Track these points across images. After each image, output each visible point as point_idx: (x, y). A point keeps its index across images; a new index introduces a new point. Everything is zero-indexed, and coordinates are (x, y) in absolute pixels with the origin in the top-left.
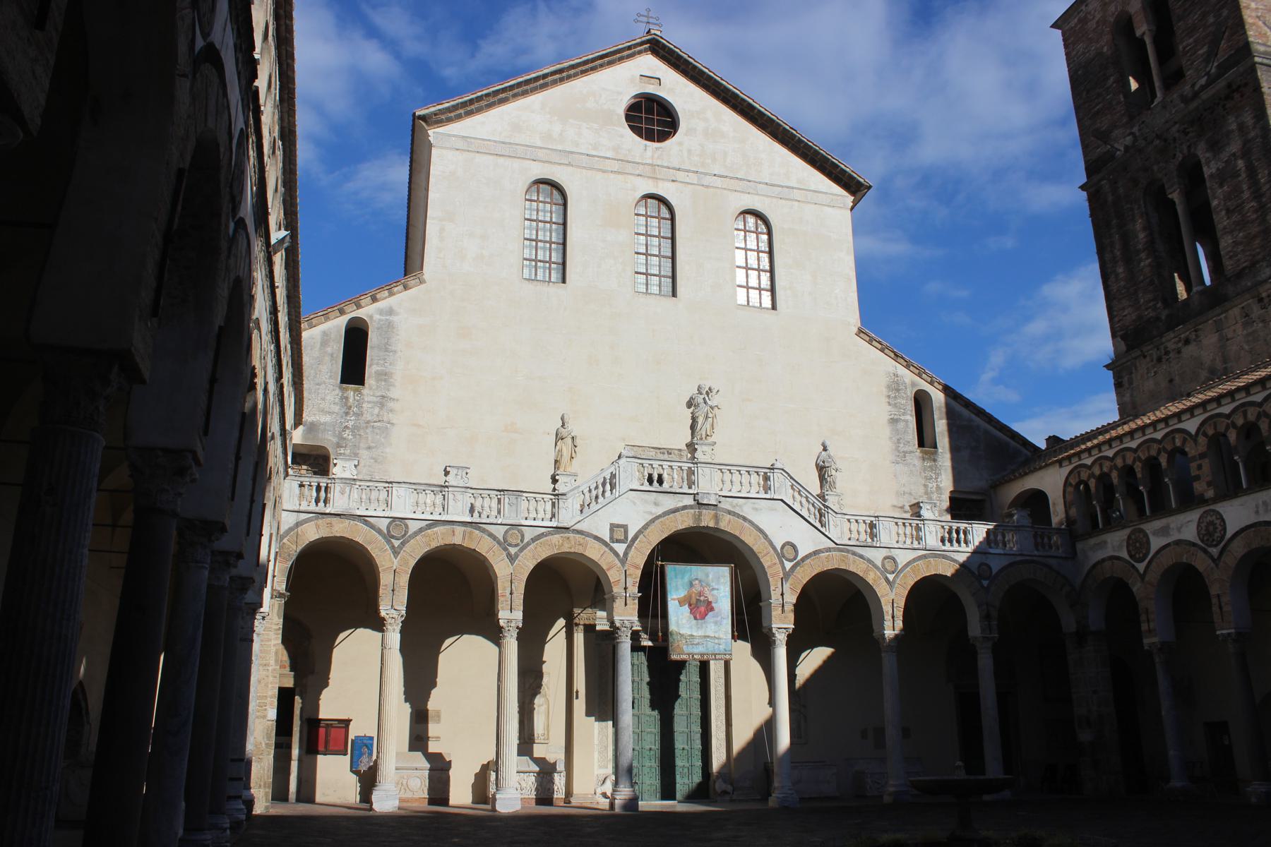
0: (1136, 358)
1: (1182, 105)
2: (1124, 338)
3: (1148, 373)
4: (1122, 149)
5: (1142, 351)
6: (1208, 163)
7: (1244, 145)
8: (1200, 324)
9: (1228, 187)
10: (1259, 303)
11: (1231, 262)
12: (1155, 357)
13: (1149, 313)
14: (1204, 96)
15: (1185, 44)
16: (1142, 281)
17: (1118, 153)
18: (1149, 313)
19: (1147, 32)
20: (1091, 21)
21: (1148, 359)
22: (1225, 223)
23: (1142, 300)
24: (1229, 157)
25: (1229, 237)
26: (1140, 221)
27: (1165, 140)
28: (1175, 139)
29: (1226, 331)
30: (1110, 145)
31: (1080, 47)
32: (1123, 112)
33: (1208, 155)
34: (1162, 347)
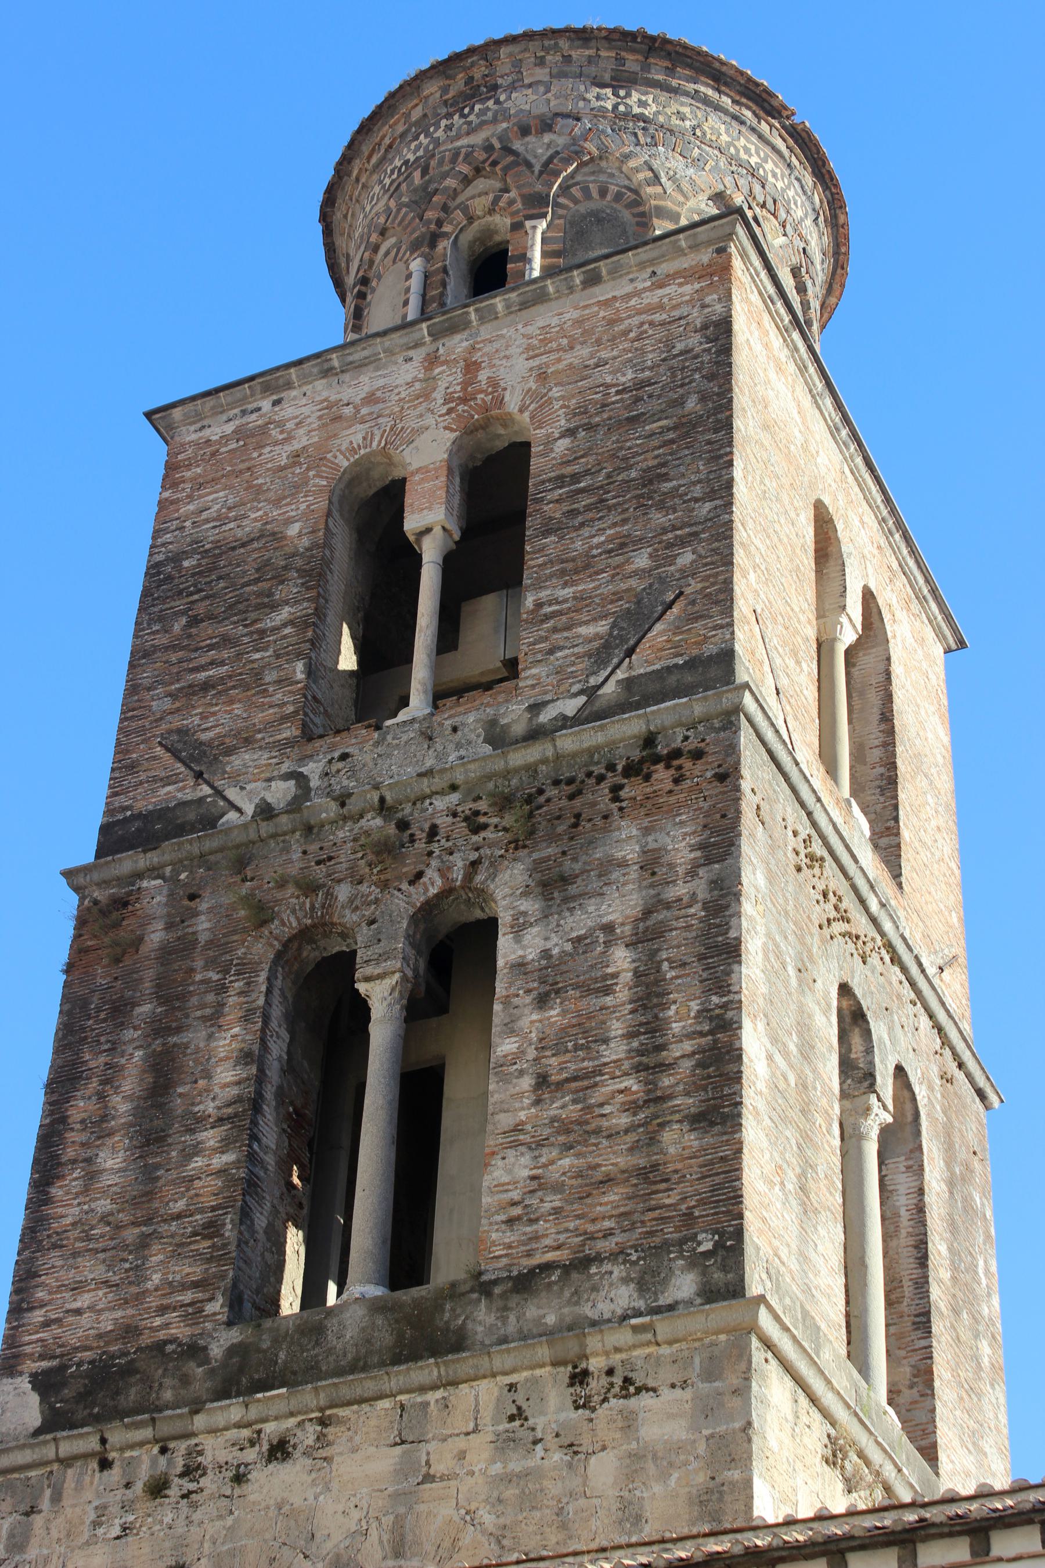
0: (67, 1462)
1: (488, 749)
2: (43, 1384)
3: (96, 1524)
4: (249, 809)
5: (103, 1441)
6: (519, 929)
7: (647, 913)
8: (349, 1403)
9: (564, 1013)
10: (571, 1385)
11: (510, 1237)
12: (143, 1474)
13: (167, 1325)
14: (568, 742)
15: (544, 594)
16: (179, 1216)
17: (232, 816)
18: (167, 1325)
19: (438, 530)
20: (276, 443)
21: (115, 1474)
22: (522, 1115)
23: (156, 1278)
24: (592, 931)
25: (526, 1160)
26: (236, 1030)
27: (403, 825)
28: (433, 832)
29: (432, 1446)
30: (212, 787)
31: (216, 499)
32: (290, 709)
33: (531, 906)
34: (181, 1447)
